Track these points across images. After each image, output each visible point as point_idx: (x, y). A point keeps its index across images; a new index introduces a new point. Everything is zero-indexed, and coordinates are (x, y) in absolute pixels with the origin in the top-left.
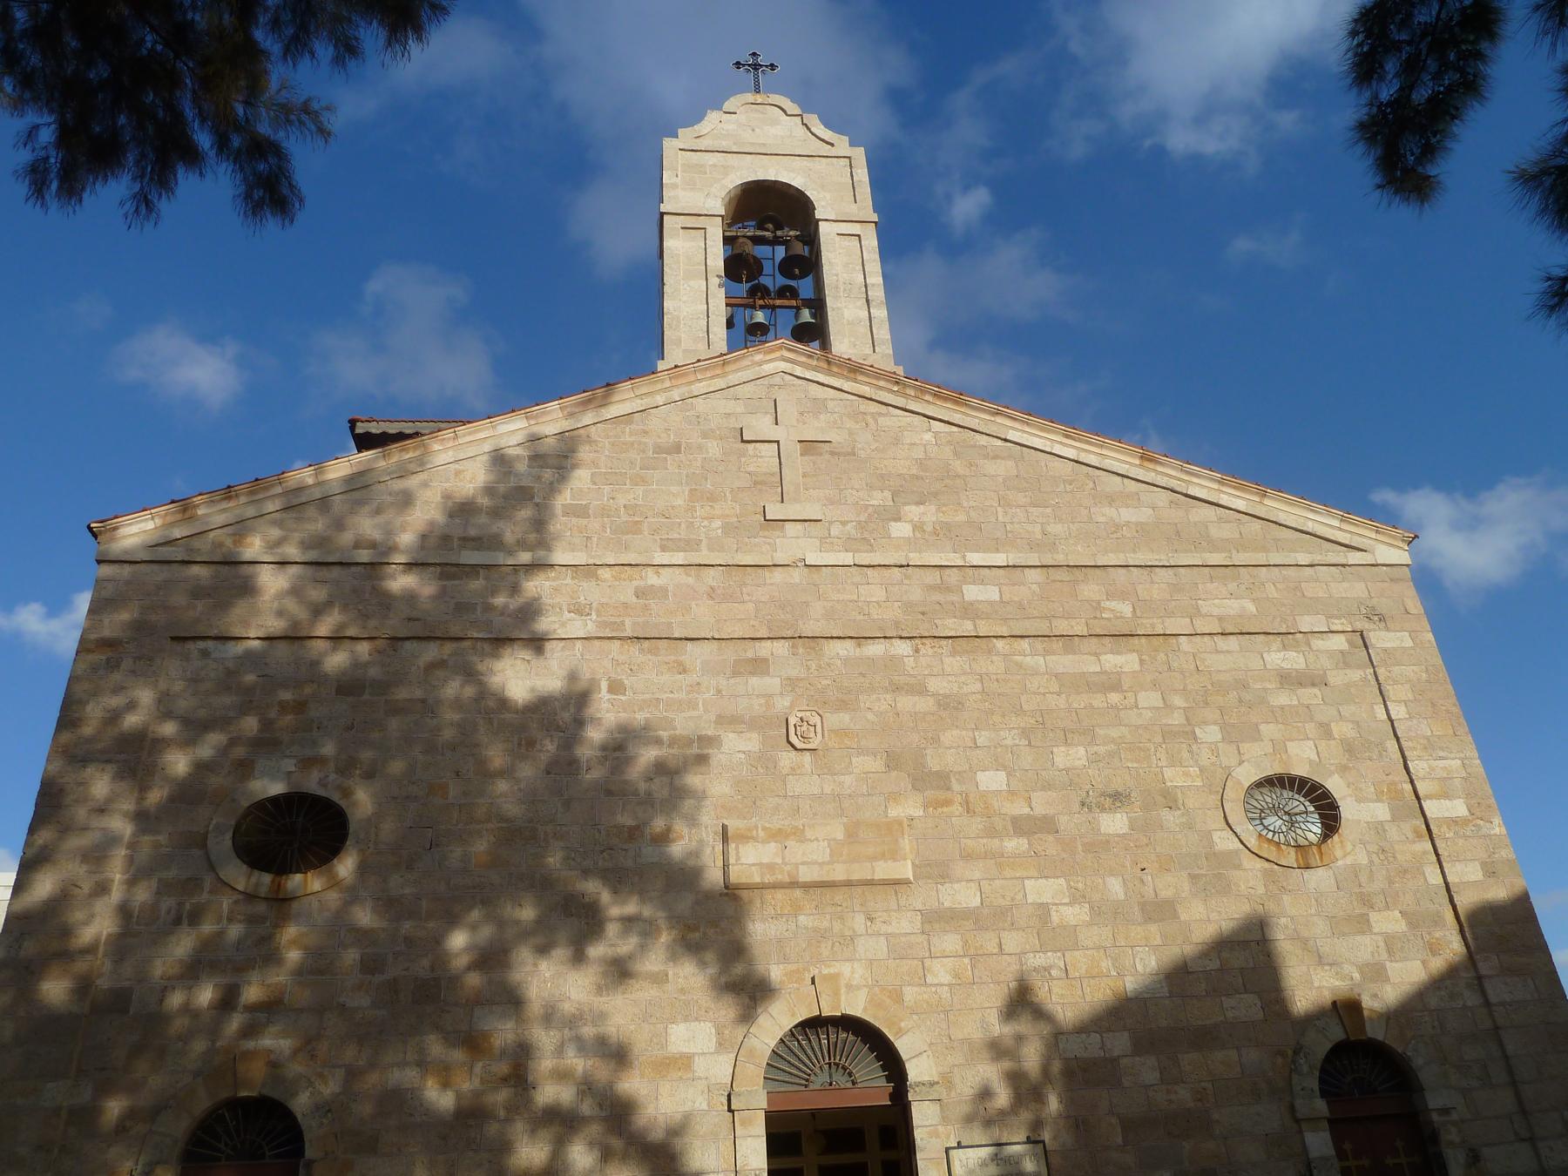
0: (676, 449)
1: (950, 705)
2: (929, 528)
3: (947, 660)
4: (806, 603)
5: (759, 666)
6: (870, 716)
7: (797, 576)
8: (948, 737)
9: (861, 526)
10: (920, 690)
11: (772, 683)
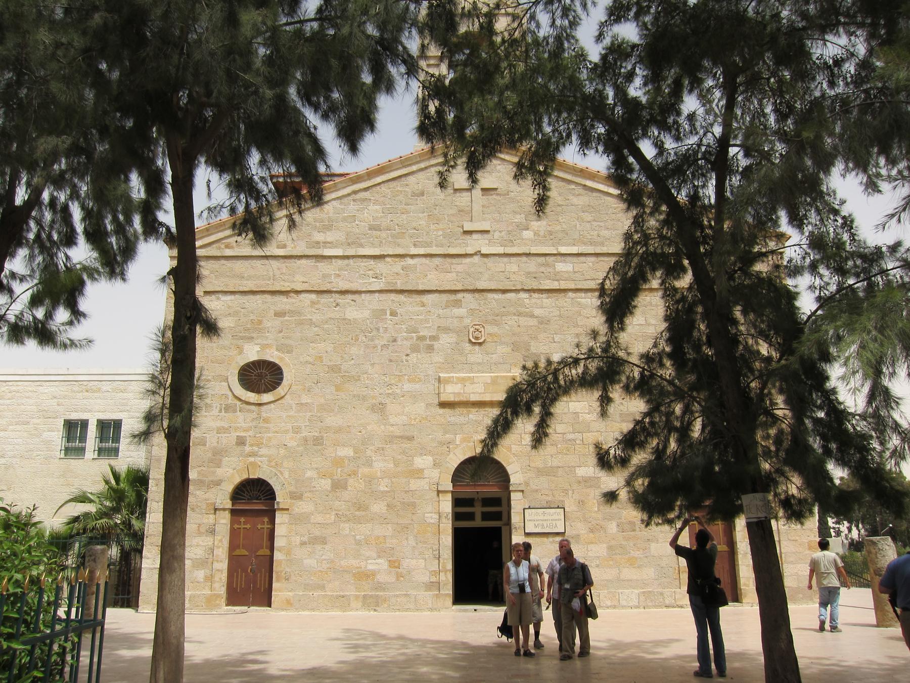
0: (422, 194)
1: (544, 322)
2: (542, 233)
3: (544, 300)
4: (481, 273)
5: (458, 304)
6: (507, 327)
7: (476, 259)
8: (542, 336)
9: (509, 232)
10: (532, 316)
11: (462, 311)
